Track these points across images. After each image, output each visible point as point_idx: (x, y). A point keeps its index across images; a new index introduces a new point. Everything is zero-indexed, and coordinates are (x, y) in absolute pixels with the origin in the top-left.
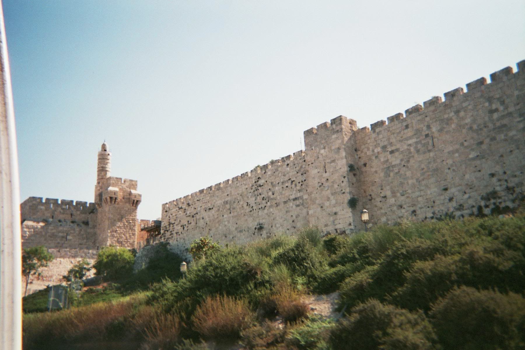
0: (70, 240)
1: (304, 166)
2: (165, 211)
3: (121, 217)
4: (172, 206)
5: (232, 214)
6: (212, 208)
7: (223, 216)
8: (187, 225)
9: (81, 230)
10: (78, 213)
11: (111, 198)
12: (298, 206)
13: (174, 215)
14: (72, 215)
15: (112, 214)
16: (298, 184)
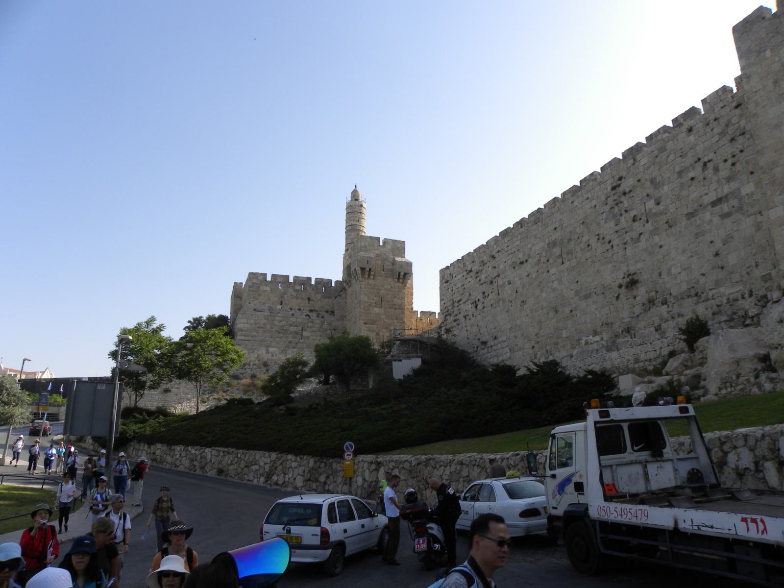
0: (308, 337)
1: (734, 120)
2: (444, 281)
3: (380, 299)
4: (456, 270)
5: (567, 264)
6: (527, 261)
7: (548, 271)
8: (482, 300)
9: (323, 323)
10: (319, 296)
11: (363, 269)
12: (725, 216)
13: (459, 285)
14: (309, 299)
15: (365, 295)
16: (721, 165)
